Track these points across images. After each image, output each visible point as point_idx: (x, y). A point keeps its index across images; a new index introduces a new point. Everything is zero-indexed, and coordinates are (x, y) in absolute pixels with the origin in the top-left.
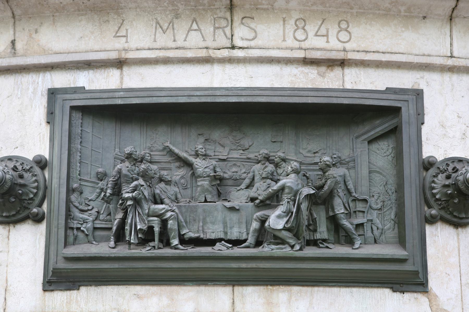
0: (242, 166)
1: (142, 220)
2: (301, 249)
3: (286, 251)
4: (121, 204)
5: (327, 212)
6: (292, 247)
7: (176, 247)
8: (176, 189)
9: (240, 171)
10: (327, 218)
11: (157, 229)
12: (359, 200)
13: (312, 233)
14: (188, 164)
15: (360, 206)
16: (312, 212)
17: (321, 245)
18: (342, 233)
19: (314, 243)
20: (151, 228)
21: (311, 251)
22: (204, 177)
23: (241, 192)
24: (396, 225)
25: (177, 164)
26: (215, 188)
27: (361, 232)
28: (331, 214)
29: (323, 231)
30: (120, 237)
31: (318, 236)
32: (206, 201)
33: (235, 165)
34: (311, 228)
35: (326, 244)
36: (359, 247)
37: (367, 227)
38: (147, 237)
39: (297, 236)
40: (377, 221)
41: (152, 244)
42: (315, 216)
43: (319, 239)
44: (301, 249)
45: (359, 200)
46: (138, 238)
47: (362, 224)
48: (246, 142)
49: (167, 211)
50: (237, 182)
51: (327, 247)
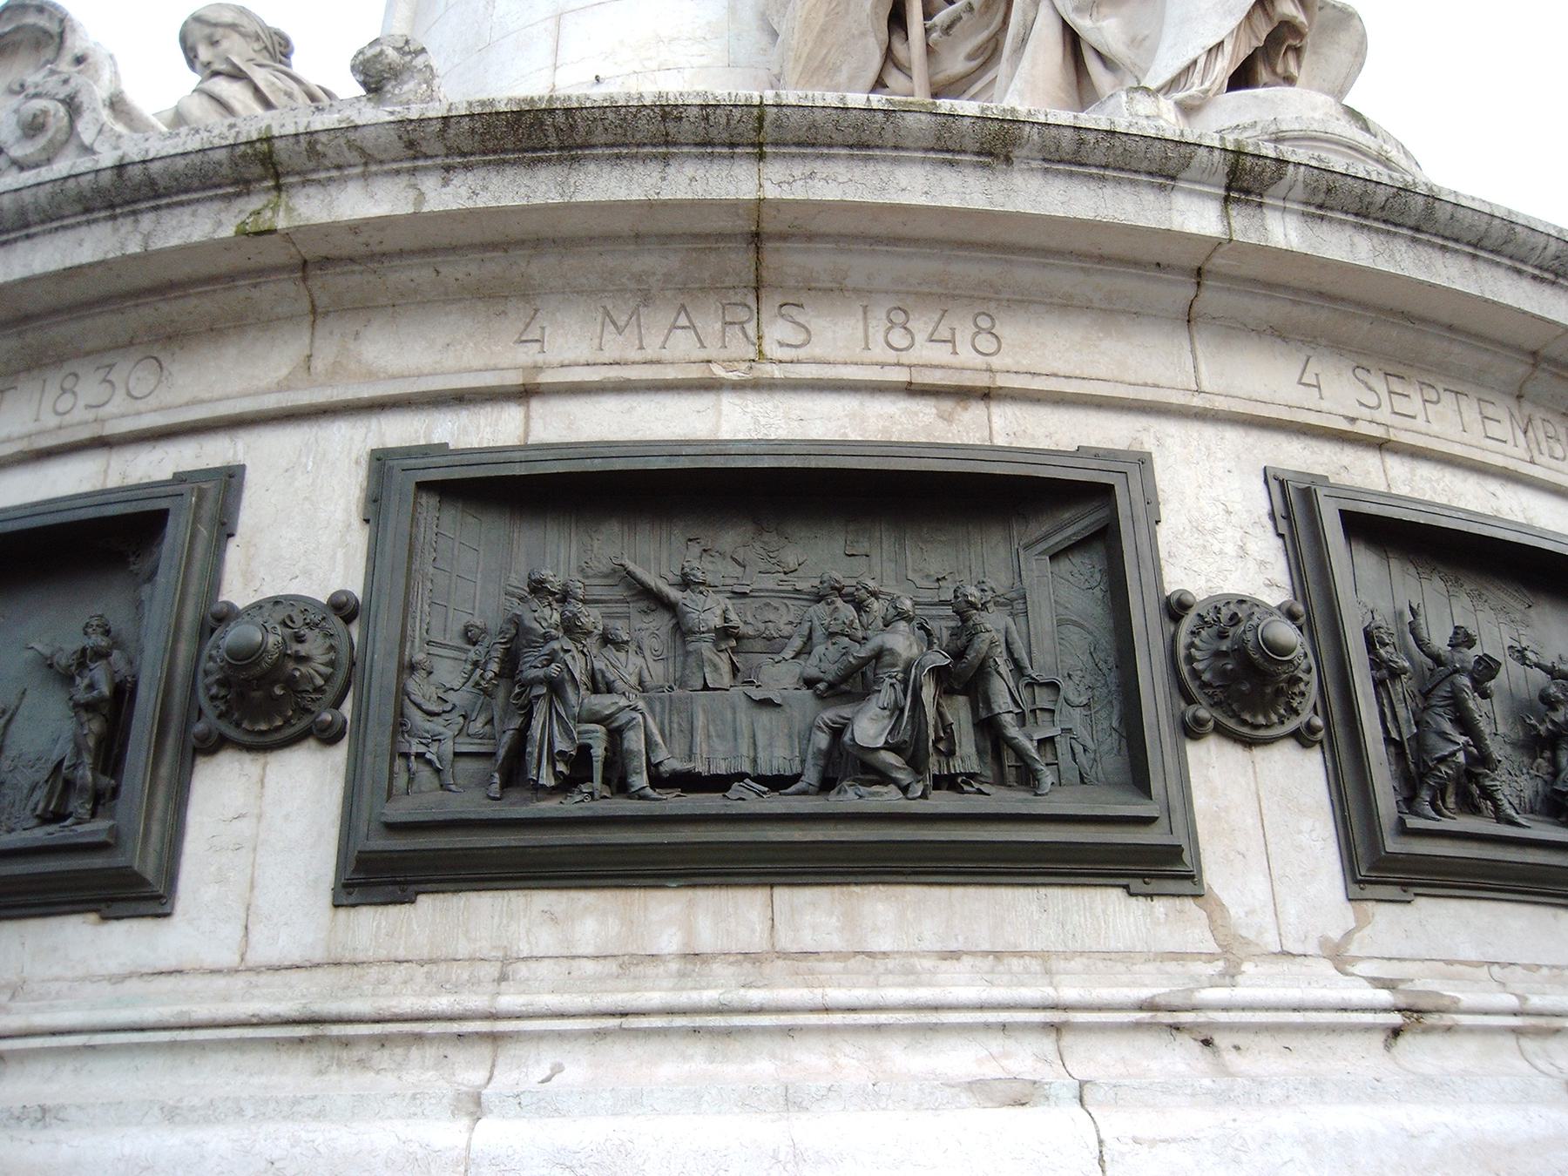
0: (783, 609)
1: (567, 732)
2: (924, 796)
3: (887, 798)
4: (519, 695)
5: (974, 710)
6: (905, 789)
8: (639, 661)
9: (782, 619)
10: (974, 725)
11: (599, 751)
12: (1041, 685)
13: (943, 759)
14: (669, 606)
15: (1043, 698)
17: (966, 788)
18: (1009, 760)
19: (948, 782)
20: (585, 750)
21: (943, 802)
23: (783, 666)
24: (1124, 742)
25: (643, 605)
26: (724, 656)
27: (1050, 759)
28: (983, 714)
29: (967, 755)
30: (514, 772)
31: (957, 766)
32: (706, 687)
33: (768, 605)
35: (976, 786)
37: (1062, 746)
38: (578, 768)
39: (916, 763)
40: (1082, 732)
41: (585, 788)
42: (950, 718)
43: (961, 774)
44: (924, 796)
45: (1041, 685)
46: (556, 774)
47: (1051, 739)
48: (791, 557)
49: (622, 709)
50: (773, 644)
51: (980, 792)
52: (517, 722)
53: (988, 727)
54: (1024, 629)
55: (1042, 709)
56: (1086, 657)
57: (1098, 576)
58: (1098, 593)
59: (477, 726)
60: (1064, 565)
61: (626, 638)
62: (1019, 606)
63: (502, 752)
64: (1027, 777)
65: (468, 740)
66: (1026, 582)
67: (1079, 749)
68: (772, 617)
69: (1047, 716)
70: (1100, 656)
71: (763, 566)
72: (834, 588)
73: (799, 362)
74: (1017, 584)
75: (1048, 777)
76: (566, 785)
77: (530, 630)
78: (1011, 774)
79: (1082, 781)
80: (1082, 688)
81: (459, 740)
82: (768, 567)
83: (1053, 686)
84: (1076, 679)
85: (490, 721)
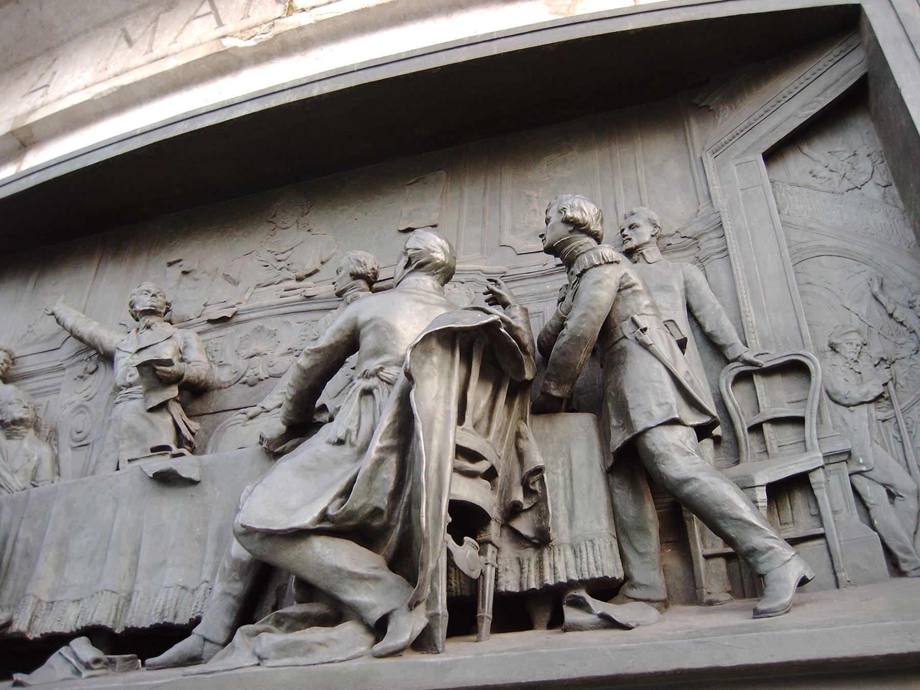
12: (768, 372)
13: (530, 554)
15: (775, 397)
16: (523, 444)
18: (704, 543)
27: (804, 525)
29: (584, 532)
31: (562, 567)
33: (259, 330)
34: (524, 525)
35: (599, 607)
36: (795, 604)
37: (831, 490)
42: (536, 458)
45: (768, 372)
47: (800, 482)
51: (609, 623)
53: (631, 464)
54: (724, 279)
55: (777, 422)
56: (866, 306)
57: (866, 165)
58: (873, 192)
60: (796, 165)
62: (710, 243)
64: (747, 577)
66: (721, 202)
67: (874, 494)
68: (261, 348)
69: (789, 432)
70: (896, 297)
72: (356, 276)
74: (704, 208)
75: (787, 567)
78: (713, 577)
79: (895, 566)
80: (865, 365)
83: (796, 368)
84: (848, 350)
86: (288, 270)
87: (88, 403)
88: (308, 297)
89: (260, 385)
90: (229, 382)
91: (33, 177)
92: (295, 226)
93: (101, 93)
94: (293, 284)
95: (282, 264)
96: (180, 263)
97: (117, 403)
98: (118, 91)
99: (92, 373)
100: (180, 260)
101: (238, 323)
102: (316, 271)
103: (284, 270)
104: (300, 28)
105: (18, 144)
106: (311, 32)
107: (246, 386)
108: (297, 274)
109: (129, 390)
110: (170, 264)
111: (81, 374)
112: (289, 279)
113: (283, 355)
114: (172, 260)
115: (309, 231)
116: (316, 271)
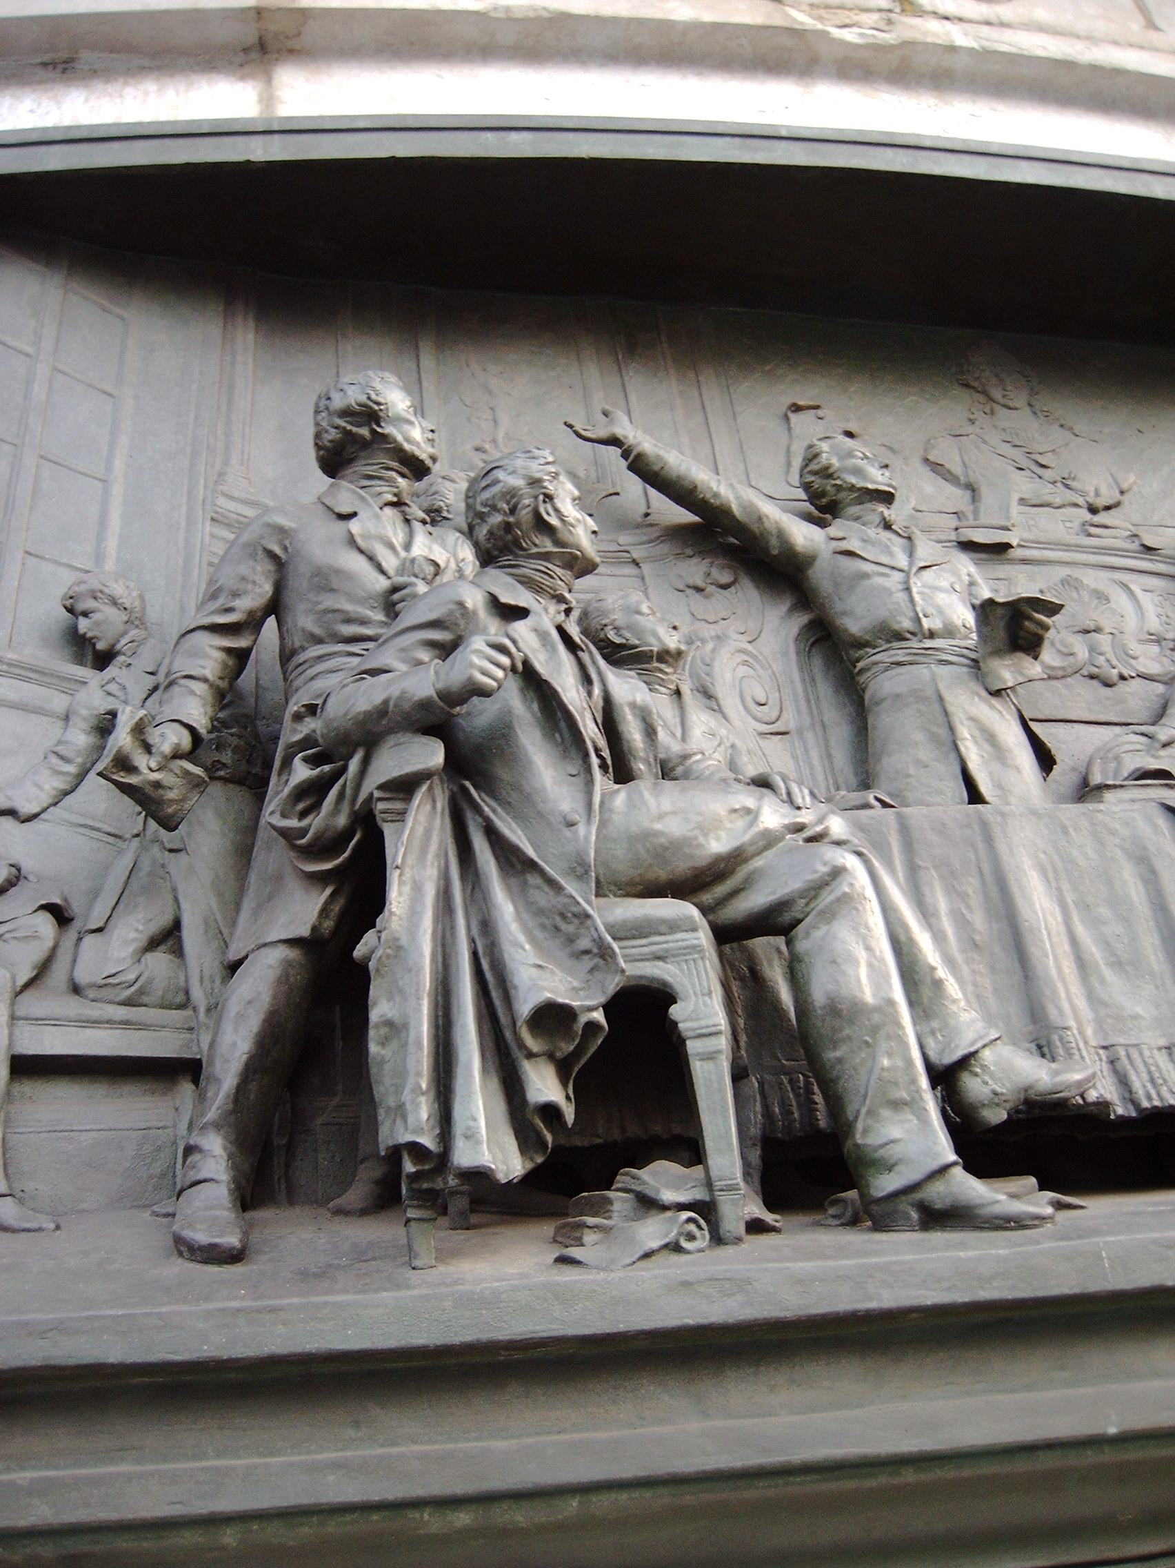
0: (1120, 600)
1: (564, 929)
4: (313, 793)
7: (937, 1193)
11: (703, 1012)
14: (776, 571)
20: (643, 1012)
22: (932, 635)
30: (305, 1111)
38: (617, 1096)
41: (666, 1180)
46: (523, 1117)
49: (769, 840)
52: (303, 910)
59: (114, 952)
61: (672, 641)
63: (233, 1046)
65: (73, 1007)
71: (1024, 485)
73: (1003, 24)
76: (565, 1181)
77: (326, 580)
81: (33, 1004)
82: (1047, 492)
85: (169, 938)
86: (1067, 486)
87: (749, 647)
88: (1149, 549)
89: (1122, 686)
90: (1063, 668)
91: (514, 136)
92: (1027, 410)
93: (508, 9)
94: (1088, 516)
95: (1047, 474)
96: (820, 413)
97: (899, 664)
98: (551, 20)
99: (725, 587)
100: (817, 407)
101: (1024, 561)
102: (1117, 505)
103: (1059, 484)
104: (952, 49)
105: (256, 40)
106: (960, 63)
107: (1095, 683)
108: (1090, 501)
109: (929, 643)
110: (797, 408)
111: (700, 583)
112: (1076, 505)
113: (1141, 641)
114: (801, 403)
115: (1062, 426)
116: (1117, 505)
